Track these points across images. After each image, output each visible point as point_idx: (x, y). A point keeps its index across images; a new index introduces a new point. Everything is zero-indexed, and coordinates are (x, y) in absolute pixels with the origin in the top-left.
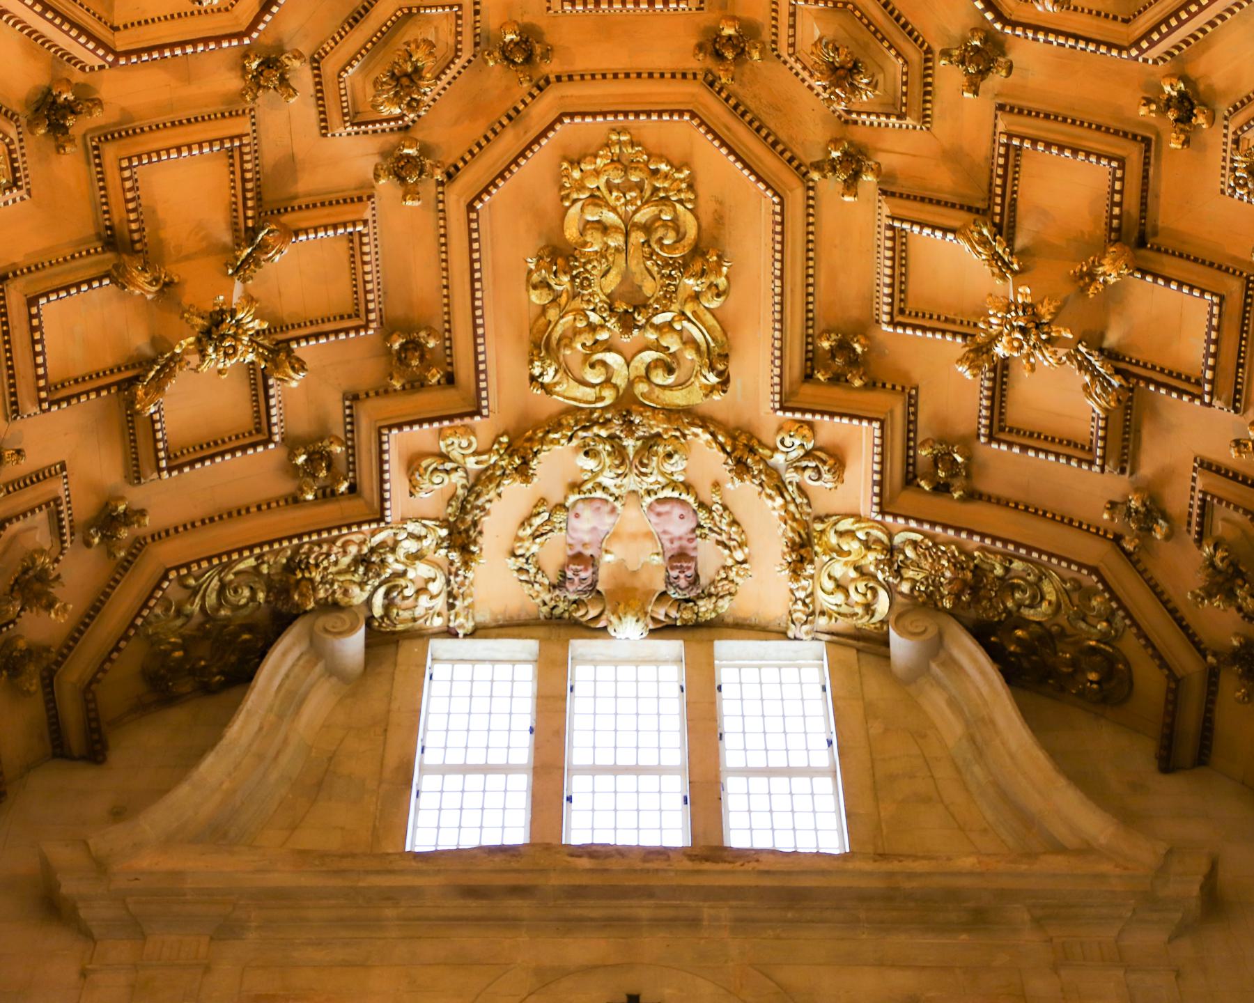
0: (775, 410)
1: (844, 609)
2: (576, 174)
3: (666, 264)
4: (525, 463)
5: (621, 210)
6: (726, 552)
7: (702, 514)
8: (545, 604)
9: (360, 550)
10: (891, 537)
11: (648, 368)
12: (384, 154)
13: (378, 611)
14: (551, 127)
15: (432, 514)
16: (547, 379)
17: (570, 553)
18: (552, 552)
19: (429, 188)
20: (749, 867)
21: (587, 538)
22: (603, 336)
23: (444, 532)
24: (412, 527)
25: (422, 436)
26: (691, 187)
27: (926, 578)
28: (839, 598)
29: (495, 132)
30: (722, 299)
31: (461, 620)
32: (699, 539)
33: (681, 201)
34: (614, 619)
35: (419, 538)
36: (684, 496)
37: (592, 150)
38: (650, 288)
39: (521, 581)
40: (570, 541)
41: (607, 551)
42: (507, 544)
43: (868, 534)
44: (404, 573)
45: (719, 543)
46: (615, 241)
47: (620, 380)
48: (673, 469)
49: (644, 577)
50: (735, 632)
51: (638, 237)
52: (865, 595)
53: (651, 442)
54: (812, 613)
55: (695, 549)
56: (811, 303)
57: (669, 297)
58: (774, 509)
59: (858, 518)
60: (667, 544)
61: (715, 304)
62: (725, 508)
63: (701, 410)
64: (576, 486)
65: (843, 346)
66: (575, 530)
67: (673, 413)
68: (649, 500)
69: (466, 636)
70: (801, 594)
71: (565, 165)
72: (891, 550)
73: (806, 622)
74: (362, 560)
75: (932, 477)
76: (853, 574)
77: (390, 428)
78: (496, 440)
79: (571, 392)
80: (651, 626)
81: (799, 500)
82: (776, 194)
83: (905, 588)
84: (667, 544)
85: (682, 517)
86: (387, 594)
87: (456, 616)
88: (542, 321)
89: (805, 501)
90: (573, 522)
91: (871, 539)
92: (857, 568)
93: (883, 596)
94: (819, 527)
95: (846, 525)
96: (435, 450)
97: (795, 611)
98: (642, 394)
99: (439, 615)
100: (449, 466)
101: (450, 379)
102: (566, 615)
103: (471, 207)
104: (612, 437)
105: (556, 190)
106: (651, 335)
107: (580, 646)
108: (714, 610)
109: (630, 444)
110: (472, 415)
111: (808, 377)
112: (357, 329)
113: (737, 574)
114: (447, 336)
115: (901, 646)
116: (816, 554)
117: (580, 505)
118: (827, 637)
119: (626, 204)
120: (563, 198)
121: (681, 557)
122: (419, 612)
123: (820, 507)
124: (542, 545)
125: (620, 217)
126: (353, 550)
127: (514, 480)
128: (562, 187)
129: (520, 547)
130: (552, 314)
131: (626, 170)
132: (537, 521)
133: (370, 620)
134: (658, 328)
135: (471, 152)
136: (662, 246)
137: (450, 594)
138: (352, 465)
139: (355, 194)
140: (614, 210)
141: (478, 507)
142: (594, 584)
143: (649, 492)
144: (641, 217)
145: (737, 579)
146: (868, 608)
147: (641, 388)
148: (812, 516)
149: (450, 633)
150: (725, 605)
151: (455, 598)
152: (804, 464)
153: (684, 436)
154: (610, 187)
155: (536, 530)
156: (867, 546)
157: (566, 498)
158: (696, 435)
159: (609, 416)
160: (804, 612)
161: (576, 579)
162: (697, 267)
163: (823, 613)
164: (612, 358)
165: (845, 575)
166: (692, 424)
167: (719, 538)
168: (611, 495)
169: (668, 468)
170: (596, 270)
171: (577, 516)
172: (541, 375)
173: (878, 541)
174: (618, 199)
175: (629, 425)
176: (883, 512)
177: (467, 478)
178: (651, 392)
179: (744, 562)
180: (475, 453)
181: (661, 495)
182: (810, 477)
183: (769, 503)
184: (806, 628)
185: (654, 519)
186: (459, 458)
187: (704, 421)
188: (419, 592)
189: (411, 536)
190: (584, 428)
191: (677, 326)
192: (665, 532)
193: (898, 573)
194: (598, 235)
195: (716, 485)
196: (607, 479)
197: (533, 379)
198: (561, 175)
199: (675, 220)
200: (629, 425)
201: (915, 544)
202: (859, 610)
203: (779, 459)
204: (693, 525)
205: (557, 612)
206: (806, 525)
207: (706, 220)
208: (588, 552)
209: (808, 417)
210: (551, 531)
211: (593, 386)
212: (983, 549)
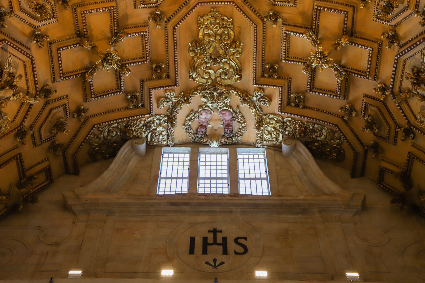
0: (254, 84)
1: (271, 139)
2: (202, 20)
3: (226, 45)
4: (188, 99)
5: (214, 30)
6: (240, 124)
8: (192, 138)
9: (144, 123)
10: (283, 119)
11: (220, 74)
12: (151, 14)
13: (149, 139)
14: (196, 6)
15: (163, 113)
16: (194, 76)
17: (199, 124)
18: (194, 124)
19: (164, 24)
20: (245, 198)
21: (204, 120)
23: (166, 118)
24: (158, 117)
25: (160, 92)
26: (232, 24)
27: (292, 130)
28: (269, 136)
29: (181, 8)
30: (240, 54)
31: (171, 142)
32: (233, 121)
33: (230, 28)
34: (211, 142)
35: (160, 120)
36: (229, 109)
37: (206, 14)
38: (221, 52)
39: (186, 132)
40: (199, 121)
41: (209, 124)
42: (183, 122)
43: (277, 119)
44: (156, 129)
45: (238, 122)
47: (213, 78)
48: (227, 102)
49: (219, 131)
50: (242, 146)
51: (218, 38)
52: (276, 135)
53: (221, 94)
54: (262, 140)
55: (232, 123)
56: (264, 56)
57: (226, 54)
58: (253, 112)
59: (275, 114)
60: (225, 122)
62: (240, 112)
63: (234, 86)
64: (201, 106)
65: (272, 67)
66: (201, 118)
68: (220, 110)
69: (172, 146)
70: (259, 135)
71: (199, 17)
72: (283, 123)
73: (260, 143)
74: (145, 125)
75: (295, 102)
76: (273, 130)
78: (180, 94)
80: (220, 144)
81: (259, 110)
82: (255, 24)
83: (287, 133)
84: (225, 122)
85: (229, 115)
86: (151, 135)
87: (169, 141)
88: (193, 61)
89: (261, 110)
90: (200, 116)
91: (278, 120)
92: (274, 128)
93: (281, 135)
94: (264, 117)
95: (272, 116)
96: (164, 96)
97: (258, 140)
98: (219, 81)
99: (165, 141)
100: (168, 100)
101: (168, 76)
102: (198, 141)
103: (174, 28)
104: (210, 93)
105: (197, 24)
107: (201, 149)
108: (237, 140)
110: (174, 86)
111: (263, 76)
113: (243, 130)
114: (168, 65)
115: (285, 147)
116: (264, 124)
117: (202, 111)
118: (266, 147)
119: (215, 29)
120: (198, 27)
121: (228, 126)
122: (160, 140)
123: (265, 112)
124: (192, 122)
125: (213, 32)
126: (143, 122)
127: (185, 104)
128: (198, 24)
129: (186, 123)
130: (195, 59)
131: (215, 19)
132: (191, 116)
133: (147, 142)
134: (223, 63)
135: (174, 14)
136: (224, 40)
137: (168, 135)
138: (142, 100)
140: (212, 30)
141: (175, 112)
142: (206, 132)
143: (220, 108)
145: (243, 132)
146: (277, 139)
148: (263, 114)
149: (168, 146)
150: (239, 138)
151: (169, 136)
152: (261, 100)
153: (230, 92)
155: (190, 118)
156: (277, 122)
157: (198, 109)
158: (233, 92)
159: (210, 87)
160: (260, 140)
161: (201, 131)
162: (234, 46)
163: (265, 140)
164: (211, 71)
165: (271, 130)
166: (232, 89)
167: (238, 120)
168: (210, 109)
171: (201, 114)
172: (192, 75)
173: (280, 120)
174: (213, 27)
175: (215, 89)
176: (281, 112)
177: (172, 104)
178: (221, 80)
179: (245, 127)
180: (174, 97)
181: (223, 109)
182: (262, 104)
183: (252, 111)
184: (260, 144)
185: (221, 115)
186: (170, 98)
187: (235, 89)
188: (160, 134)
189: (158, 119)
190: (203, 90)
192: (224, 119)
193: (285, 129)
194: (208, 37)
195: (238, 106)
196: (209, 104)
197: (190, 76)
198: (198, 20)
199: (228, 32)
200: (215, 89)
201: (289, 121)
202: (274, 139)
204: (231, 117)
205: (196, 140)
206: (261, 117)
207: (236, 33)
208: (204, 124)
209: (262, 86)
210: (194, 118)
211: (206, 79)
212: (307, 122)
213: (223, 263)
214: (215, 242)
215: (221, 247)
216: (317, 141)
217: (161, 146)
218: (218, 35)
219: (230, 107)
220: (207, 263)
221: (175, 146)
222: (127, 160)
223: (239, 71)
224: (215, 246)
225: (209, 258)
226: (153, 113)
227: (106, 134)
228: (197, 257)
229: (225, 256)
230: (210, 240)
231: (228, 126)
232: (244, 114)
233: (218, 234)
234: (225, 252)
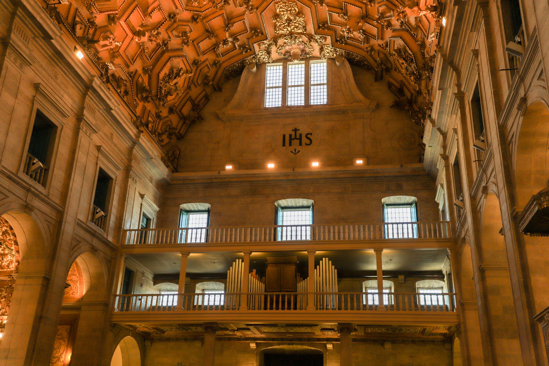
2: (277, 5)
11: (294, 28)
28: (328, 54)
38: (292, 18)
46: (285, 13)
61: (303, 19)
67: (298, 33)
77: (254, 43)
79: (281, 32)
95: (328, 46)
106: (293, 24)
112: (246, 33)
130: (277, 23)
139: (243, 14)
140: (284, 9)
144: (289, 9)
146: (333, 56)
147: (293, 31)
170: (283, 17)
187: (304, 34)
213: (299, 151)
214: (296, 138)
215: (298, 141)
217: (265, 63)
219: (303, 42)
221: (273, 62)
222: (246, 80)
224: (296, 140)
225: (292, 148)
230: (293, 137)
231: (303, 51)
234: (300, 144)
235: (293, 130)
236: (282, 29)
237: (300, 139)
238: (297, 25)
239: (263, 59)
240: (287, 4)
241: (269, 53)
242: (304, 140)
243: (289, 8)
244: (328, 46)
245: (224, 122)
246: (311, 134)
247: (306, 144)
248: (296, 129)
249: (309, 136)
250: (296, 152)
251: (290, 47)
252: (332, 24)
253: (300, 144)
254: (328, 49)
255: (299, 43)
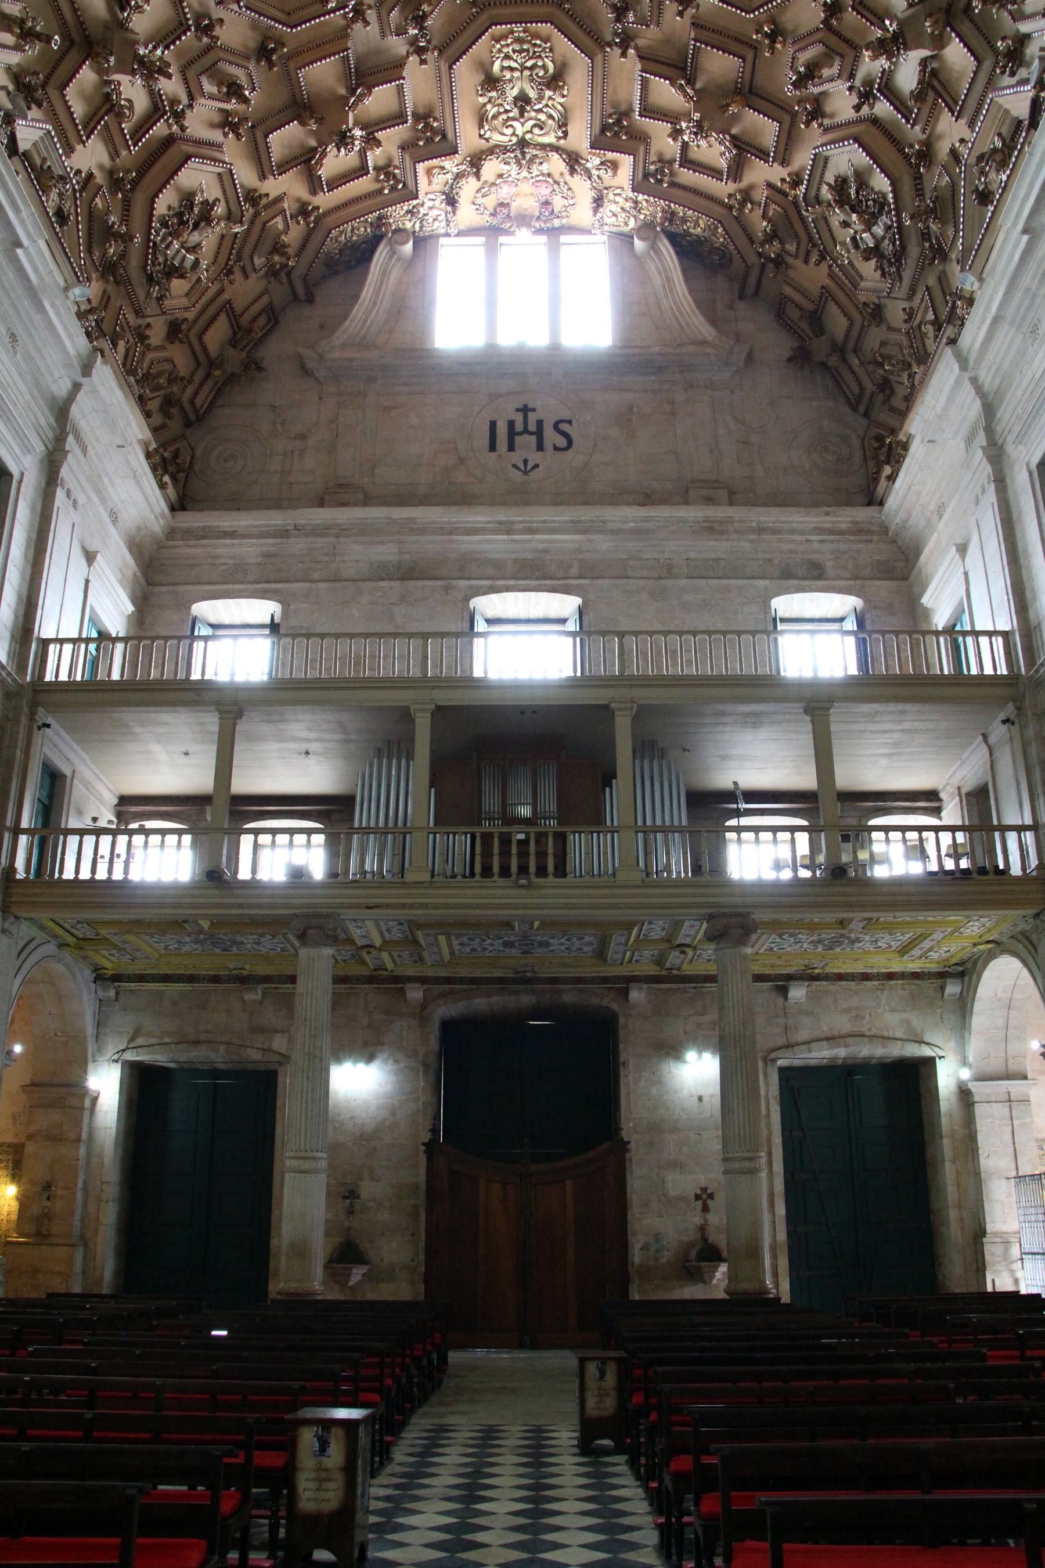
2: (498, 46)
7: (556, 186)
16: (487, 136)
22: (511, 115)
28: (614, 219)
38: (532, 94)
46: (517, 74)
47: (520, 135)
53: (531, 161)
57: (540, 98)
59: (622, 188)
61: (562, 100)
67: (543, 147)
68: (531, 181)
79: (497, 138)
92: (622, 208)
95: (618, 191)
106: (533, 114)
109: (524, 162)
121: (547, 203)
123: (607, 184)
130: (489, 107)
140: (516, 61)
144: (529, 64)
146: (626, 224)
147: (528, 136)
150: (564, 221)
154: (514, 51)
169: (540, 168)
191: (545, 110)
195: (562, 174)
200: (523, 153)
203: (589, 165)
213: (537, 466)
214: (526, 431)
216: (691, 235)
217: (438, 236)
218: (526, 68)
220: (515, 466)
221: (460, 234)
222: (385, 273)
223: (563, 125)
224: (526, 437)
225: (517, 457)
226: (421, 194)
227: (349, 234)
228: (500, 456)
229: (540, 453)
230: (519, 427)
232: (571, 185)
233: (530, 414)
234: (540, 447)
235: (518, 410)
236: (499, 127)
237: (539, 433)
238: (542, 117)
239: (435, 220)
240: (525, 47)
241: (451, 201)
242: (551, 437)
243: (531, 58)
244: (618, 191)
245: (319, 382)
246: (570, 422)
247: (556, 448)
248: (525, 406)
249: (564, 427)
250: (529, 468)
251: (514, 190)
252: (646, 117)
253: (540, 447)
254: (616, 203)
255: (541, 178)
